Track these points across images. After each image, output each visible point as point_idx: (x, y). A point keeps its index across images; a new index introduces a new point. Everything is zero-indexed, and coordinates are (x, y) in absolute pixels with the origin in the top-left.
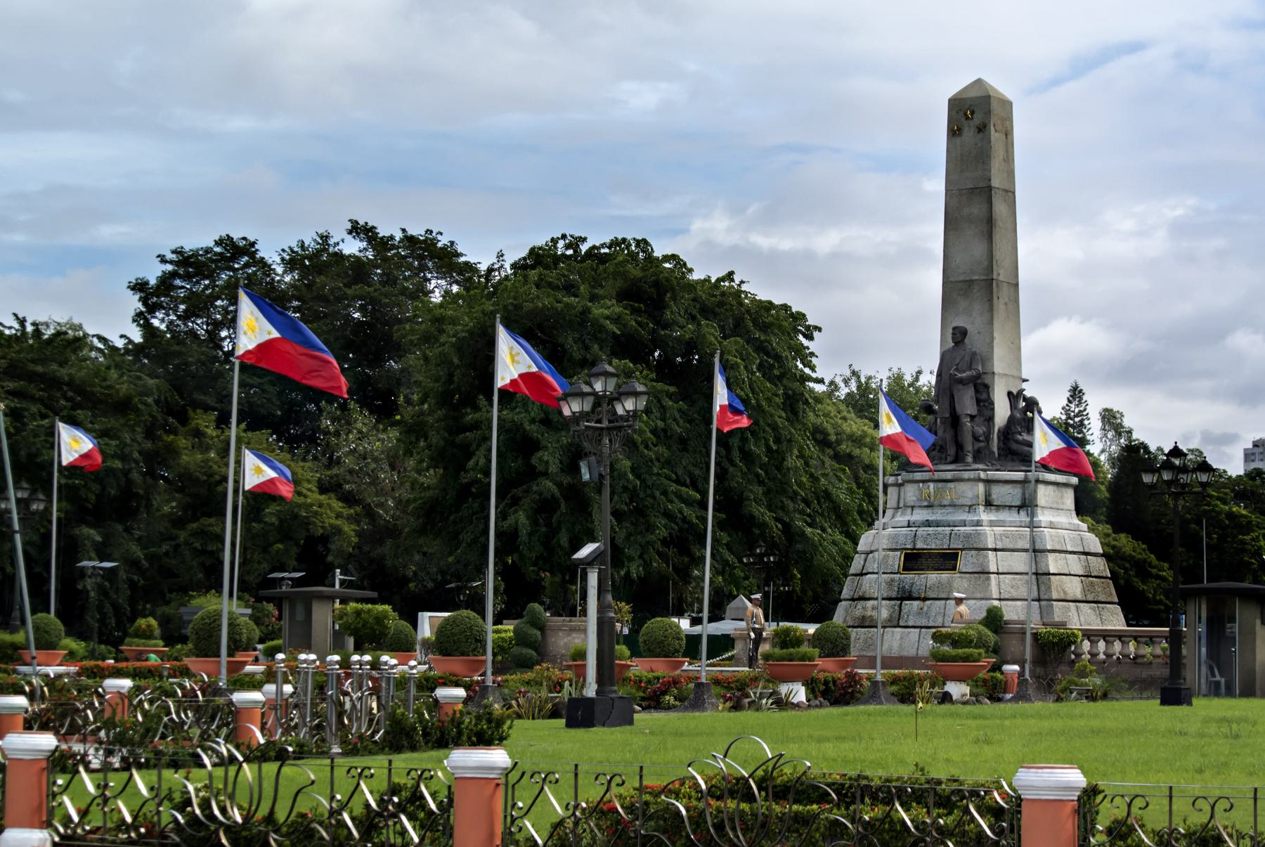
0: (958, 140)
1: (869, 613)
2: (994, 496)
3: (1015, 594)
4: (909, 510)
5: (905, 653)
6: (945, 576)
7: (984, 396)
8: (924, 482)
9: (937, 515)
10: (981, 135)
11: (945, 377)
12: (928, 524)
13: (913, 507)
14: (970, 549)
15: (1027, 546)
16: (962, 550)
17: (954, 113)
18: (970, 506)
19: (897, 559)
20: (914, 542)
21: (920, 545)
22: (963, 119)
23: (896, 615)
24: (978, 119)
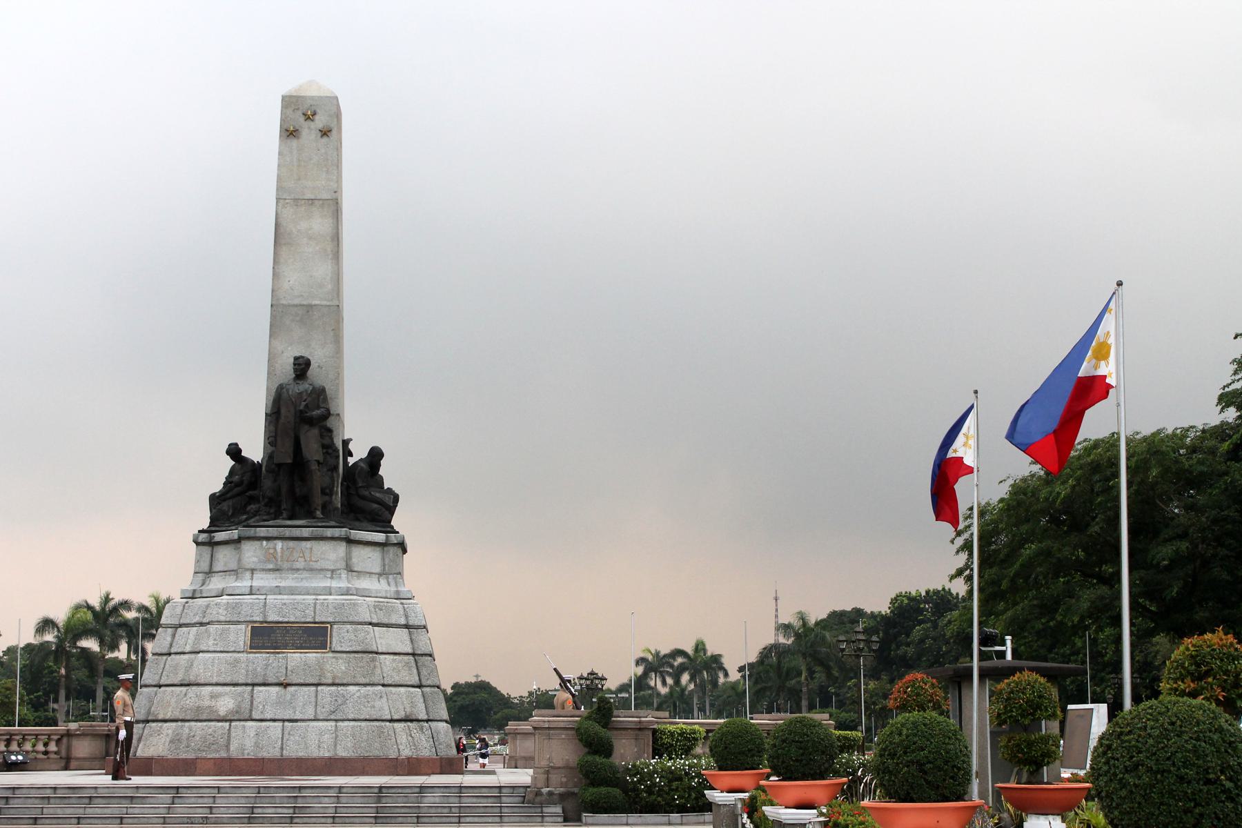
0: (294, 143)
1: (207, 703)
2: (354, 560)
3: (397, 679)
4: (248, 574)
5: (265, 755)
6: (312, 656)
7: (327, 441)
8: (268, 539)
9: (288, 581)
10: (325, 139)
11: (287, 414)
12: (278, 590)
13: (253, 571)
14: (344, 623)
15: (403, 621)
16: (332, 624)
17: (289, 112)
18: (333, 571)
19: (241, 635)
20: (264, 613)
21: (272, 617)
22: (302, 119)
23: (246, 705)
24: (320, 121)
